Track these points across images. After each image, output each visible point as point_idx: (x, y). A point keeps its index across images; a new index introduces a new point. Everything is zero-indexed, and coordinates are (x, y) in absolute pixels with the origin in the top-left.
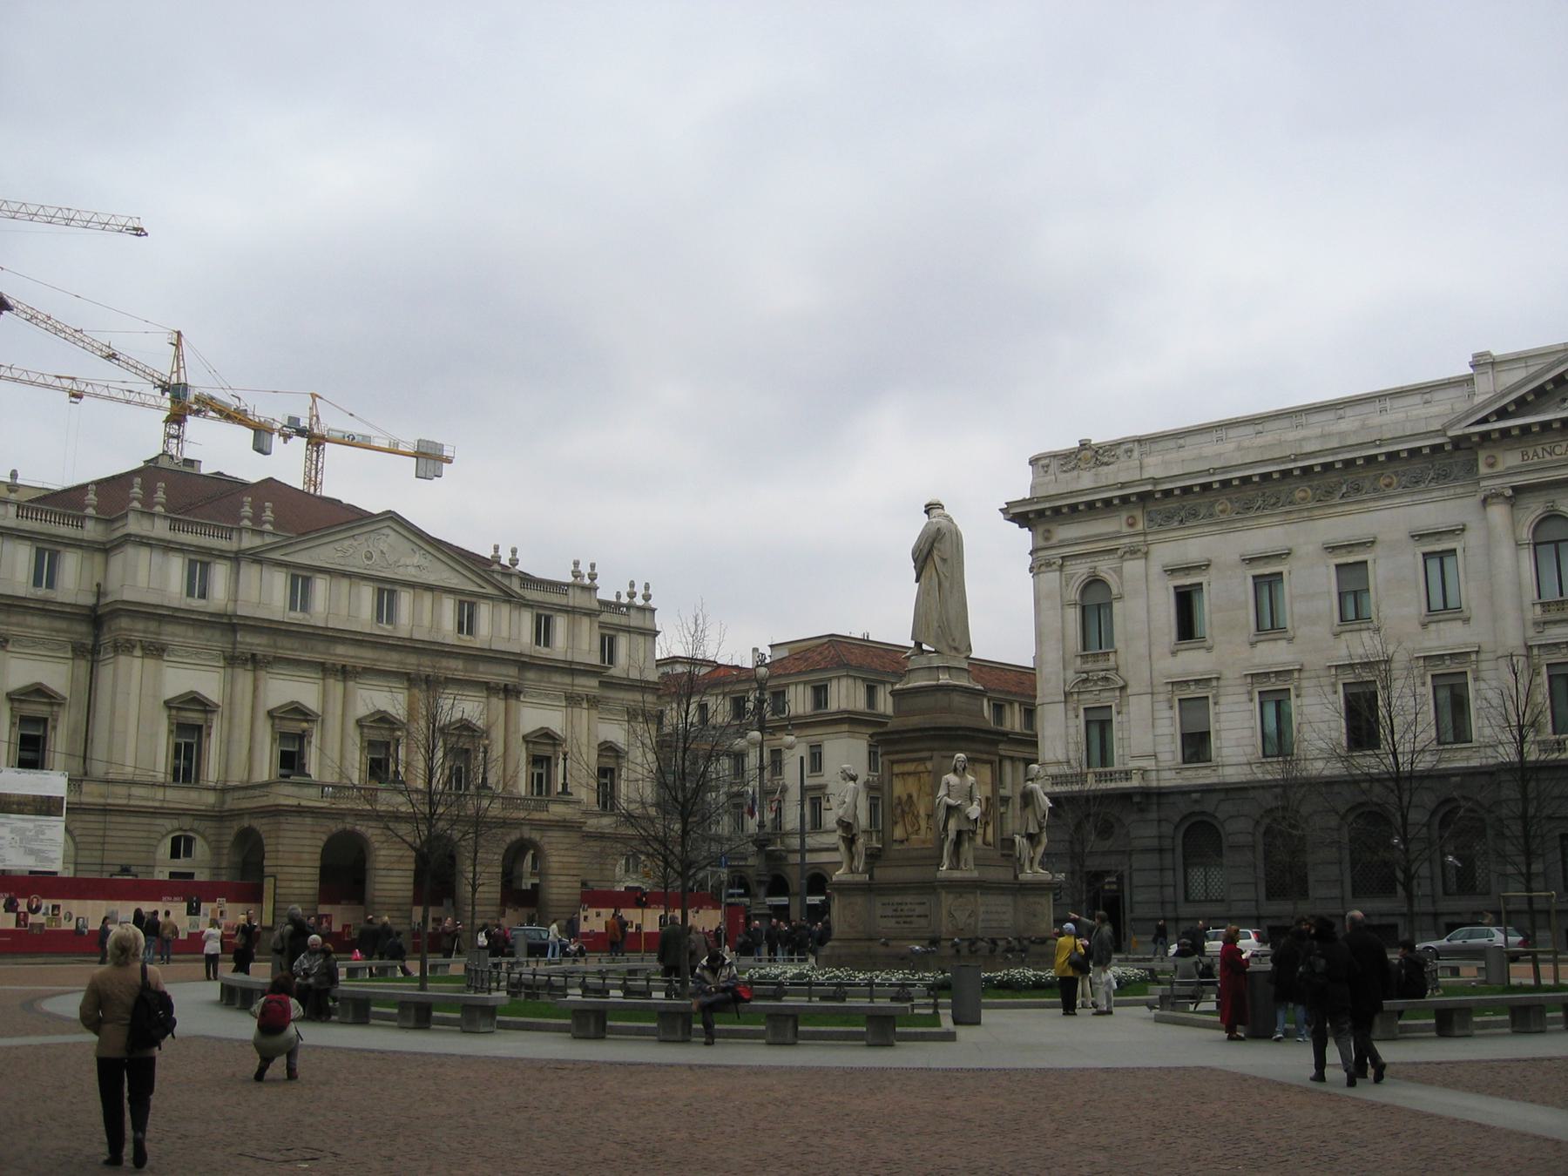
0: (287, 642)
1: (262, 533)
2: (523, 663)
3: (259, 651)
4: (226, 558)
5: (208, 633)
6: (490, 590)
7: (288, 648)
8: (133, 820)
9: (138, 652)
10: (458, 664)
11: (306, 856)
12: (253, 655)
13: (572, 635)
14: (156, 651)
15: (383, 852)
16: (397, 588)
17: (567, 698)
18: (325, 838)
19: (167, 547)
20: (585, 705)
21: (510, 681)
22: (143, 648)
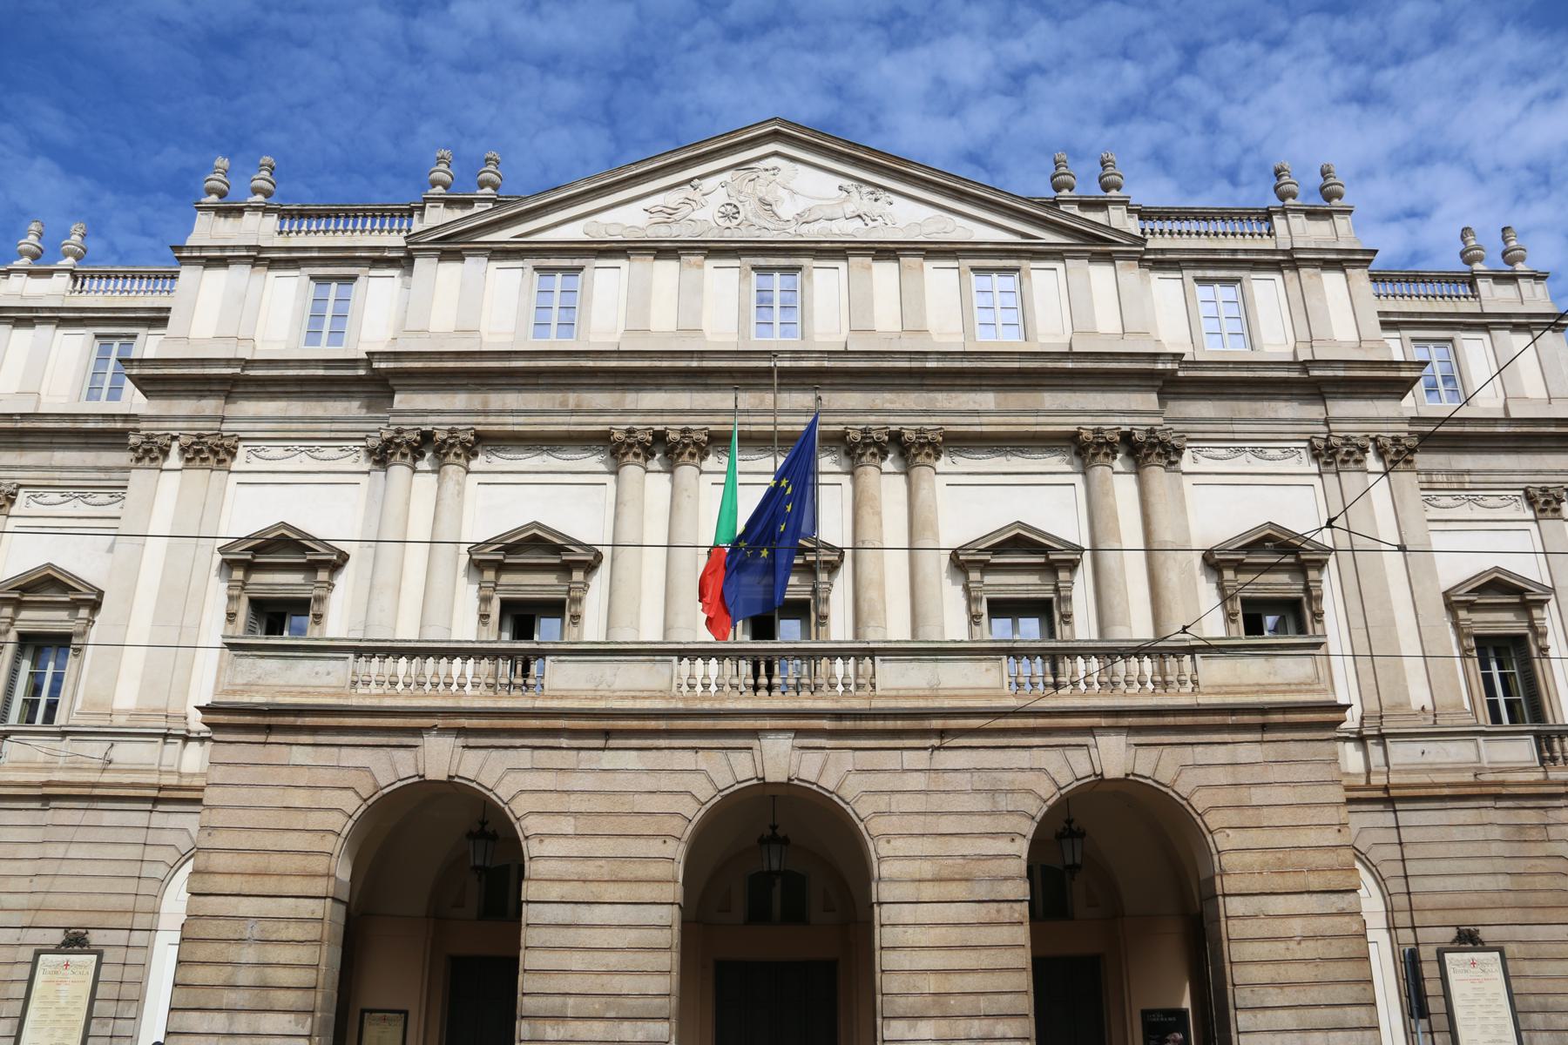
0: (512, 400)
1: (468, 203)
2: (1170, 380)
3: (440, 427)
4: (391, 263)
5: (336, 408)
6: (1049, 237)
7: (512, 407)
8: (109, 818)
9: (174, 460)
10: (986, 400)
11: (277, 862)
12: (427, 437)
13: (1303, 310)
14: (211, 452)
15: (551, 847)
16: (805, 262)
17: (1316, 454)
18: (352, 804)
19: (259, 258)
20: (1372, 462)
21: (1139, 426)
22: (183, 450)
